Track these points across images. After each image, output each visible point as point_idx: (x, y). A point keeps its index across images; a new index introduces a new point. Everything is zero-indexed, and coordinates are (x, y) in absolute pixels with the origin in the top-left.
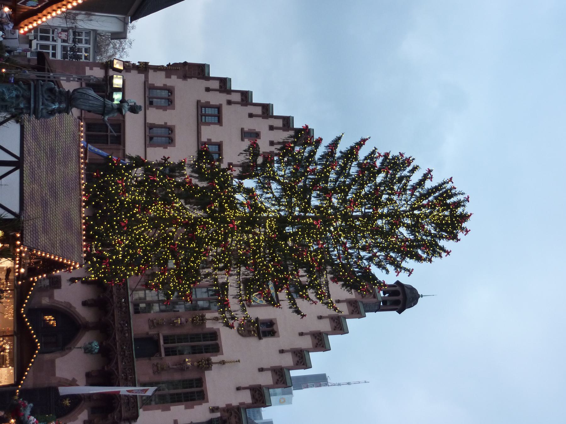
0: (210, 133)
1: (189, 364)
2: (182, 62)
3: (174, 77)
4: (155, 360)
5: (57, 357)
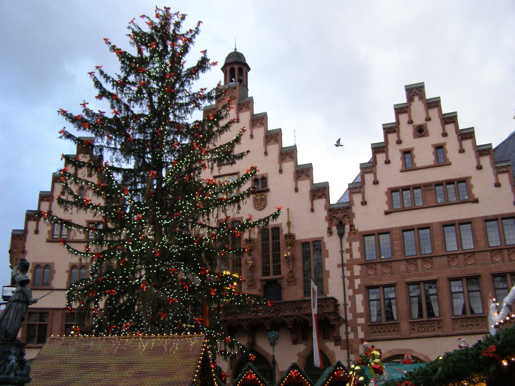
1: (289, 254)
2: (9, 255)
4: (284, 284)
5: (278, 369)
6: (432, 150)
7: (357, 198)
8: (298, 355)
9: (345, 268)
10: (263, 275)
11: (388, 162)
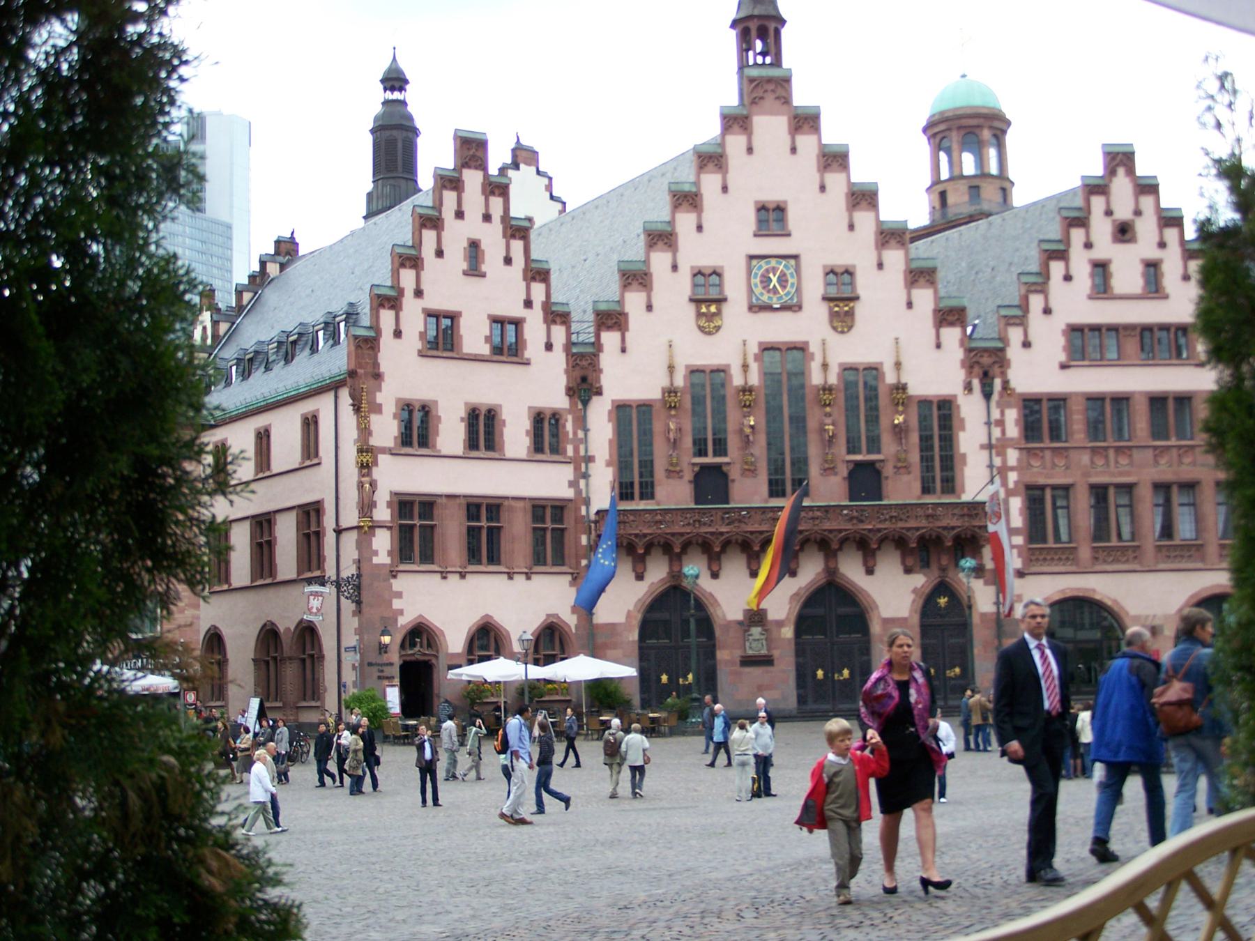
0: (474, 336)
3: (380, 398)
4: (888, 471)
6: (1139, 268)
7: (1015, 335)
8: (915, 591)
9: (994, 452)
10: (849, 452)
11: (1068, 278)
